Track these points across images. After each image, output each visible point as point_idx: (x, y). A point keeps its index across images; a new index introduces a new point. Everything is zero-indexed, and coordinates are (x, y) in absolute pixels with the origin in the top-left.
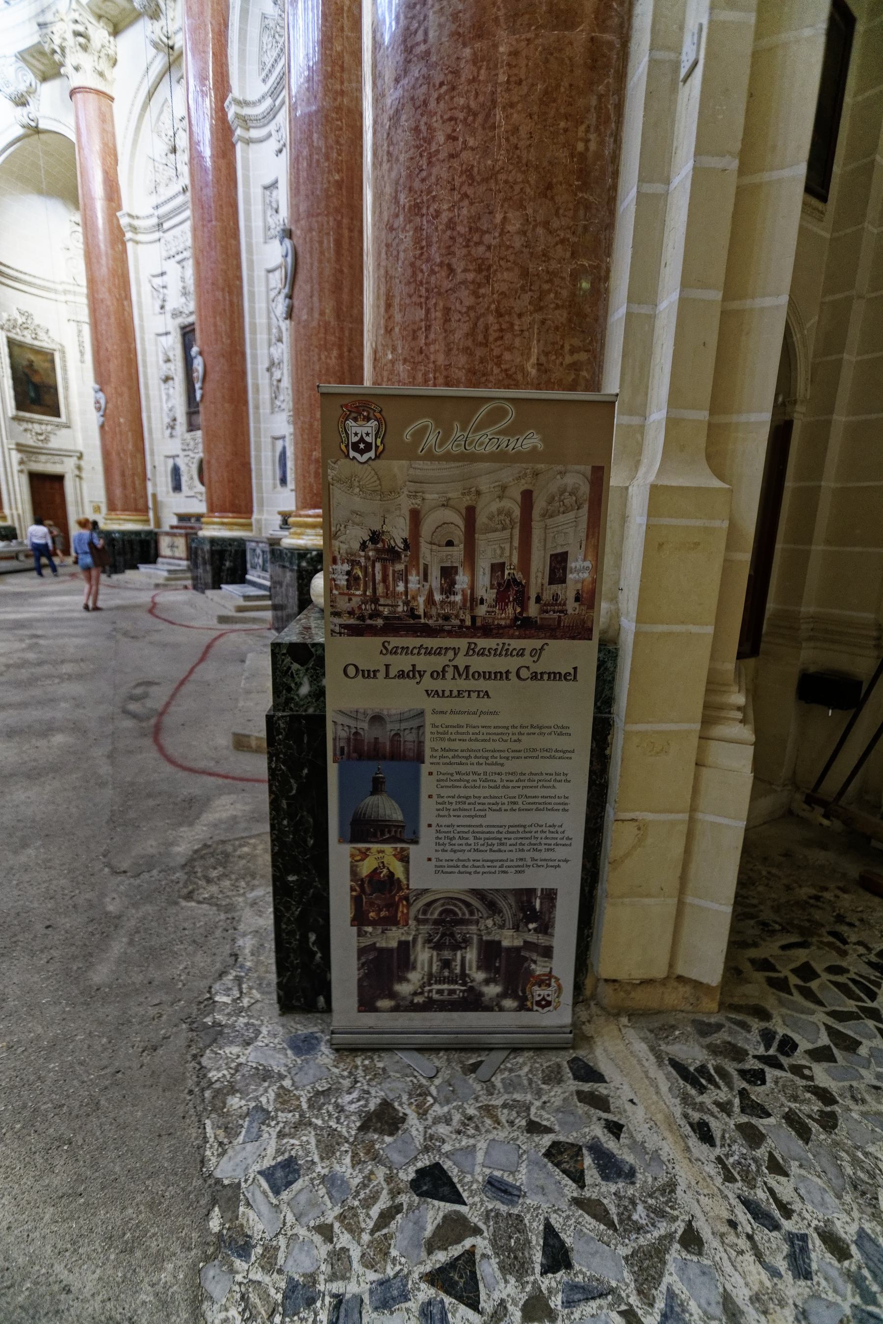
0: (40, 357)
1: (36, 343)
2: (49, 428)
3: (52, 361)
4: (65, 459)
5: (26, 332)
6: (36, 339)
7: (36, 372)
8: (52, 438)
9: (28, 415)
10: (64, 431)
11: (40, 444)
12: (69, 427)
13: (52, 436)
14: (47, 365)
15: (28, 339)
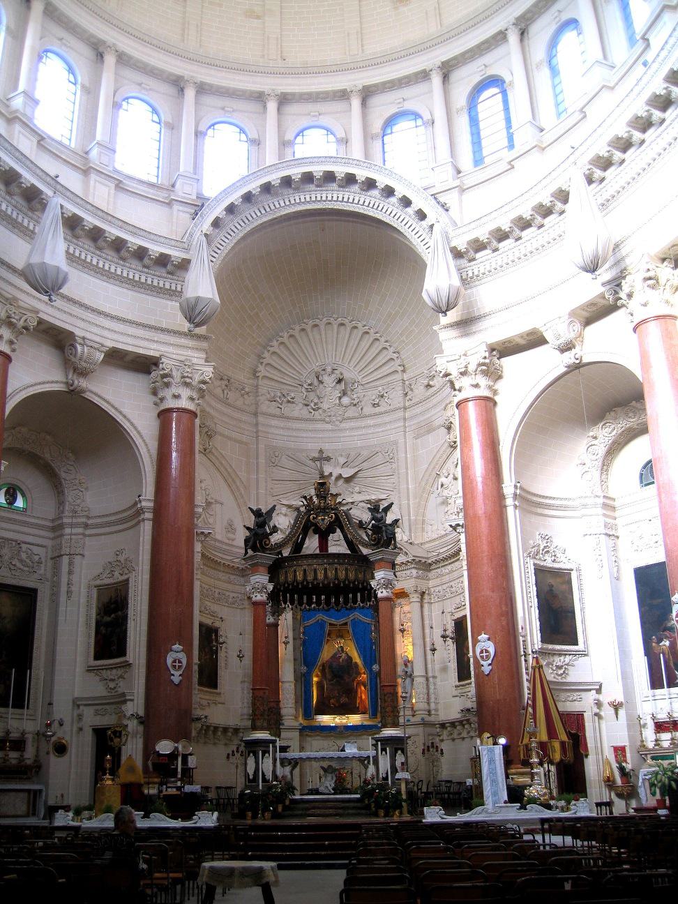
0: (559, 580)
1: (556, 565)
2: (568, 659)
3: (569, 582)
4: (583, 694)
5: (547, 557)
6: (554, 561)
7: (555, 596)
8: (571, 671)
9: (550, 647)
10: (582, 660)
11: (560, 679)
12: (585, 655)
13: (569, 668)
14: (564, 587)
15: (548, 563)
